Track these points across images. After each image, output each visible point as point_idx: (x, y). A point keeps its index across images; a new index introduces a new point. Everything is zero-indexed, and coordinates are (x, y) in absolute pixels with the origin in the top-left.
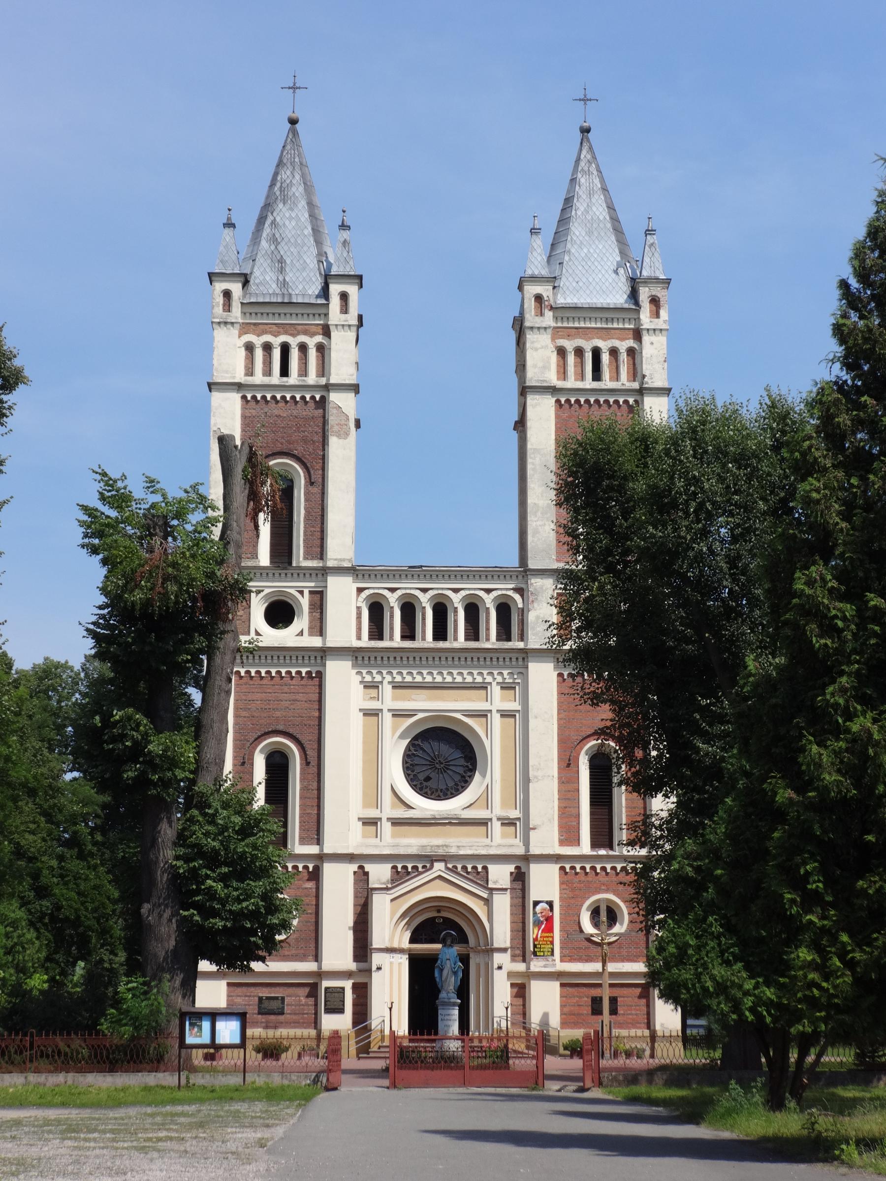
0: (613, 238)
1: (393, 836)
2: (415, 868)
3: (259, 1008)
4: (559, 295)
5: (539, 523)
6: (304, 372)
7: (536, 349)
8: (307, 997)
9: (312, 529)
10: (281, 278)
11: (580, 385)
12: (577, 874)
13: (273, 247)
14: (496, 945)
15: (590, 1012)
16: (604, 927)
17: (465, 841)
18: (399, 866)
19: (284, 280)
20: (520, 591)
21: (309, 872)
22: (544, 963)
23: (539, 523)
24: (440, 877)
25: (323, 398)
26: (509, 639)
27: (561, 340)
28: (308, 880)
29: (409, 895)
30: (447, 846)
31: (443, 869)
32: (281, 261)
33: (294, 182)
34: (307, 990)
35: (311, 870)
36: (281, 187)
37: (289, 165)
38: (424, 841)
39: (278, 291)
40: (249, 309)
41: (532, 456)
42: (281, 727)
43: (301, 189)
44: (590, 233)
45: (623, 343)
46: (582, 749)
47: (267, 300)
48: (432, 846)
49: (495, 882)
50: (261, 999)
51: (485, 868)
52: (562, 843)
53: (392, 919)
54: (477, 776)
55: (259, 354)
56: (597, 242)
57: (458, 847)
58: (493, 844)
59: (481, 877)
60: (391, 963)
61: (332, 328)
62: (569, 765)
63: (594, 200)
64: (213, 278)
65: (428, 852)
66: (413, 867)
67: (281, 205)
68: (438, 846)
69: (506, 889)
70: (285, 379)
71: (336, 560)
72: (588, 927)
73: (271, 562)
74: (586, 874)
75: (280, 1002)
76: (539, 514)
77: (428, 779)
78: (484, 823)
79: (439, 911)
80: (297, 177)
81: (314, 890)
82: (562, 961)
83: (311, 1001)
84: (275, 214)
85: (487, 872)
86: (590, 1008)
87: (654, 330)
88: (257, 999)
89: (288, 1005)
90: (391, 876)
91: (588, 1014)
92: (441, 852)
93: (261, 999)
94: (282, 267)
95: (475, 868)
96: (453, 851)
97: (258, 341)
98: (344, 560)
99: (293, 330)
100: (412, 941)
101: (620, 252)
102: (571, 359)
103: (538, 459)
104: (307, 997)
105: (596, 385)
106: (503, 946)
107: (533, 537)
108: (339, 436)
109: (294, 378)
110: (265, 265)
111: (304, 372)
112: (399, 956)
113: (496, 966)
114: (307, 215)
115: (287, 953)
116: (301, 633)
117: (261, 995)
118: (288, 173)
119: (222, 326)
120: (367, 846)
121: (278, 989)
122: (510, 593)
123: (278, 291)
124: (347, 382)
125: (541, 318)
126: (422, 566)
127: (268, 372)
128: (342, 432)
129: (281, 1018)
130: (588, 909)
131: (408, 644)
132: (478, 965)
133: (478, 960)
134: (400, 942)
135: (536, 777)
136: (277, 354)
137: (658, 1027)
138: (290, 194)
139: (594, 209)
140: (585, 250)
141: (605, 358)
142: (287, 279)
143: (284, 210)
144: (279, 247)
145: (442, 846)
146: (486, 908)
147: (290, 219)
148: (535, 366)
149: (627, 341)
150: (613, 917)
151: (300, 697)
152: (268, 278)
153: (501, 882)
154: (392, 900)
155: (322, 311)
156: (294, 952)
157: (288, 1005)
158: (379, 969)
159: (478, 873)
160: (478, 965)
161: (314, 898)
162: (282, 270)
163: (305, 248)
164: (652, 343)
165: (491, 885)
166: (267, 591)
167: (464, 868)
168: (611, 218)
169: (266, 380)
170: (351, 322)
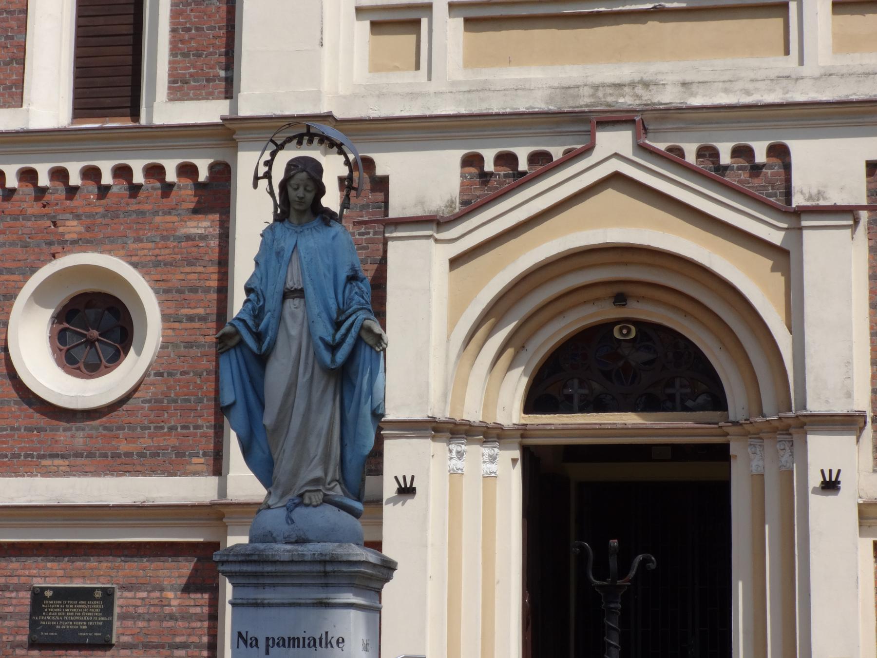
1: (472, 60)
2: (539, 159)
3: (33, 625)
8: (187, 589)
14: (815, 406)
18: (489, 155)
21: (199, 186)
24: (616, 180)
28: (196, 211)
30: (646, 85)
31: (628, 152)
34: (186, 567)
35: (203, 175)
48: (596, 87)
50: (38, 596)
51: (780, 152)
53: (452, 323)
57: (684, 84)
58: (807, 70)
60: (456, 475)
65: (584, 101)
66: (533, 158)
68: (619, 86)
69: (850, 211)
75: (97, 605)
79: (620, 299)
81: (214, 243)
83: (199, 602)
85: (787, 167)
88: (26, 597)
89: (123, 617)
90: (462, 192)
92: (626, 101)
93: (38, 596)
95: (743, 152)
96: (669, 96)
100: (533, 404)
104: (187, 589)
106: (839, 407)
112: (486, 451)
113: (815, 480)
115: (124, 447)
117: (39, 583)
120: (381, 96)
121: (93, 563)
133: (756, 464)
134: (489, 402)
145: (632, 85)
146: (779, 279)
154: (455, 262)
156: (145, 442)
157: (123, 617)
158: (406, 491)
159: (756, 169)
161: (214, 269)
165: (798, 201)
167: (708, 153)
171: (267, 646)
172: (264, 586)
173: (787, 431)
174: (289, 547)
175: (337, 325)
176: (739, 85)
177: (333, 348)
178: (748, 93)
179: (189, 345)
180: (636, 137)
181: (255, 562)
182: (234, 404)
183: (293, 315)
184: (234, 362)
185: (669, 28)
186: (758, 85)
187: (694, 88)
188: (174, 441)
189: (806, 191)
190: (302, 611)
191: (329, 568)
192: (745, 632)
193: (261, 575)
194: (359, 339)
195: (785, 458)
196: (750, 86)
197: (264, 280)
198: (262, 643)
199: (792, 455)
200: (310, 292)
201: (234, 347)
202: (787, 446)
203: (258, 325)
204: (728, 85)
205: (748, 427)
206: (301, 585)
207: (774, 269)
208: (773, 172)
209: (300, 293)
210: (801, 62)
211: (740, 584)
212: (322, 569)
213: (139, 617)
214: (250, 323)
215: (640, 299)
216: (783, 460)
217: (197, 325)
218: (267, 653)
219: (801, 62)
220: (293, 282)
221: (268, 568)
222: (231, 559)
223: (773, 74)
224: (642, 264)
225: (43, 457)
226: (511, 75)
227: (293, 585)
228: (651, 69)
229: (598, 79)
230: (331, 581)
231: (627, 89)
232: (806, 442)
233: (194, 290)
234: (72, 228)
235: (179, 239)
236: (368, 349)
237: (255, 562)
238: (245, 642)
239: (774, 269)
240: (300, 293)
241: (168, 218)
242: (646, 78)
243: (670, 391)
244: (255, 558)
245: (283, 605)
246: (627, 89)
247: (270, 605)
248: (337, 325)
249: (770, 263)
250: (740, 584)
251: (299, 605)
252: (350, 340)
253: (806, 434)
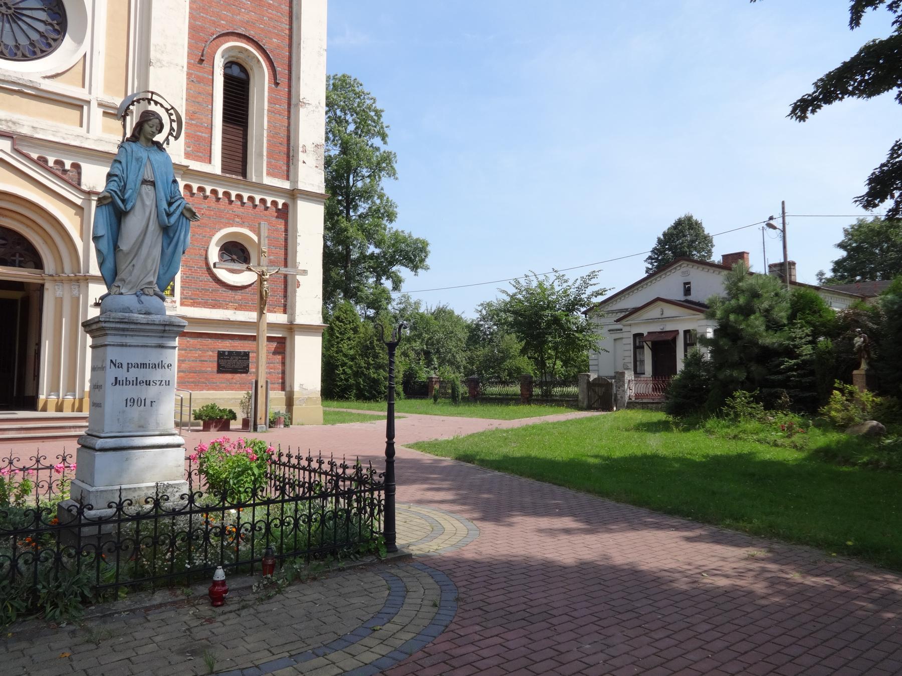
12: (206, 197)
15: (215, 369)
17: (42, 123)
30: (14, 123)
31: (8, 150)
46: (218, 47)
51: (76, 166)
54: (67, 41)
59: (73, 178)
62: (201, 61)
74: (218, 199)
78: (78, 105)
82: (182, 304)
85: (79, 174)
86: (216, 365)
91: (213, 372)
96: (25, 131)
130: (217, 245)
132: (59, 302)
133: (59, 293)
135: (159, 61)
137: (296, 388)
145: (6, 121)
146: (78, 219)
160: (59, 302)
171: (128, 367)
172: (126, 335)
173: (78, 281)
174: (143, 316)
175: (170, 204)
177: (169, 215)
178: (64, 138)
180: (13, 145)
181: (126, 322)
182: (102, 236)
183: (147, 194)
184: (105, 213)
185: (25, 101)
186: (69, 136)
187: (38, 130)
189: (88, 185)
190: (149, 349)
191: (167, 328)
192: (48, 361)
193: (127, 330)
194: (182, 214)
195: (75, 292)
196: (65, 136)
197: (125, 172)
198: (125, 366)
199: (79, 291)
200: (159, 184)
201: (105, 205)
202: (76, 287)
203: (123, 195)
204: (55, 133)
205: (57, 278)
206: (148, 336)
207: (76, 214)
208: (73, 174)
209: (153, 184)
210: (88, 132)
211: (47, 342)
212: (163, 328)
214: (119, 193)
216: (74, 293)
218: (128, 371)
219: (88, 132)
220: (149, 176)
221: (132, 326)
222: (111, 320)
224: (11, 202)
227: (144, 336)
228: (15, 117)
230: (165, 335)
231: (3, 122)
232: (88, 286)
236: (184, 219)
237: (126, 322)
238: (115, 365)
239: (76, 214)
240: (153, 184)
242: (14, 120)
243: (14, 258)
244: (126, 320)
245: (138, 346)
246: (3, 122)
247: (130, 346)
248: (170, 204)
249: (74, 211)
250: (47, 342)
251: (147, 346)
252: (178, 213)
253: (88, 283)
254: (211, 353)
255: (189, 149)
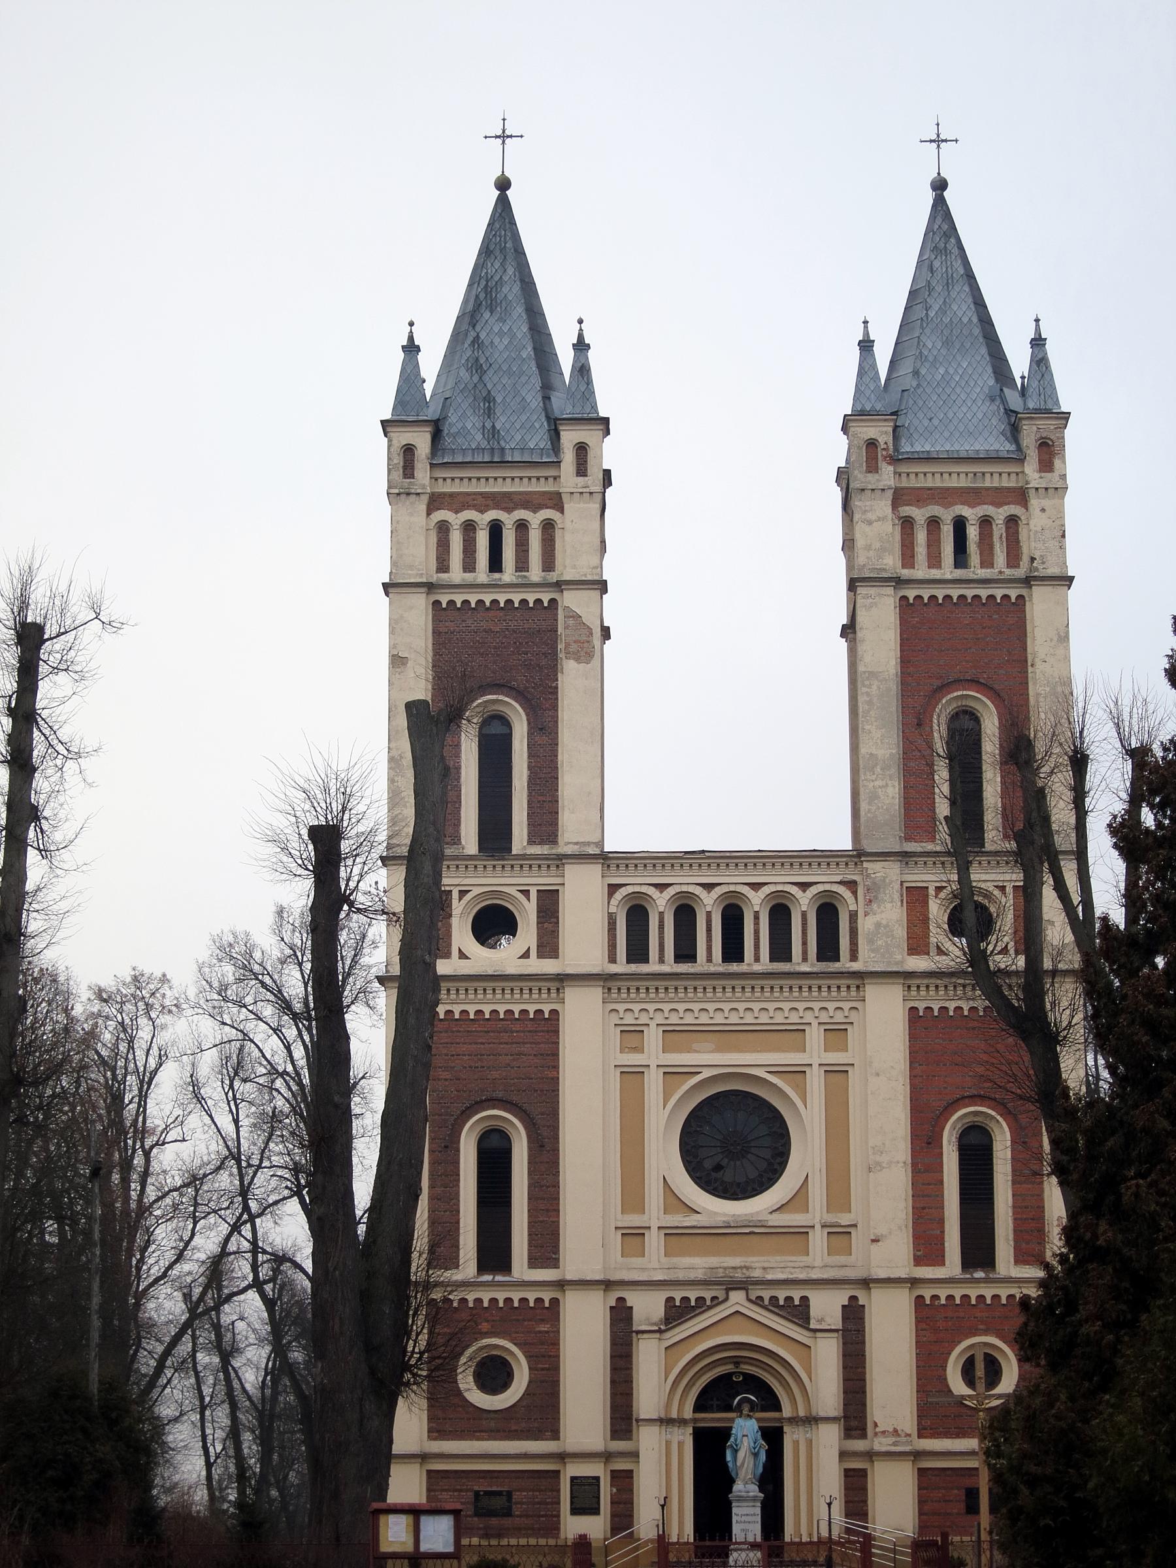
0: (984, 350)
3: (476, 1507)
4: (903, 441)
5: (877, 783)
6: (522, 564)
7: (870, 523)
9: (540, 798)
10: (488, 425)
11: (935, 574)
13: (476, 378)
16: (981, 1385)
17: (774, 1260)
19: (493, 426)
20: (851, 885)
22: (894, 1439)
23: (877, 783)
25: (553, 601)
26: (646, 960)
27: (907, 508)
29: (691, 1340)
30: (747, 1268)
32: (489, 399)
33: (506, 278)
36: (487, 285)
37: (497, 253)
38: (713, 1261)
39: (484, 444)
40: (440, 473)
41: (867, 683)
42: (500, 1094)
43: (516, 288)
44: (947, 343)
45: (1001, 510)
46: (947, 1120)
47: (469, 459)
48: (725, 1268)
49: (820, 1321)
50: (477, 1494)
51: (805, 1299)
52: (918, 1261)
55: (456, 540)
56: (959, 357)
57: (764, 1268)
59: (799, 1313)
61: (565, 498)
63: (953, 294)
64: (389, 429)
67: (487, 315)
70: (497, 575)
71: (576, 843)
72: (959, 1387)
73: (481, 849)
75: (505, 1498)
76: (878, 770)
77: (718, 1168)
78: (802, 1233)
80: (510, 271)
84: (478, 328)
87: (1046, 489)
88: (471, 1495)
92: (739, 1275)
94: (489, 407)
96: (757, 1274)
97: (456, 520)
98: (588, 844)
99: (507, 501)
100: (699, 1407)
101: (995, 372)
102: (921, 536)
103: (875, 687)
105: (959, 573)
107: (869, 804)
108: (578, 660)
109: (509, 574)
110: (465, 405)
111: (522, 564)
114: (525, 328)
116: (526, 955)
117: (476, 1488)
118: (497, 265)
119: (403, 497)
120: (629, 1269)
122: (835, 888)
123: (484, 444)
124: (589, 578)
125: (876, 476)
126: (703, 852)
127: (469, 565)
128: (582, 654)
129: (507, 1522)
131: (634, 968)
132: (796, 1443)
133: (795, 1437)
136: (483, 540)
138: (500, 297)
139: (954, 306)
140: (942, 370)
141: (972, 532)
142: (498, 426)
143: (492, 321)
144: (486, 378)
145: (741, 1268)
147: (501, 334)
148: (868, 548)
149: (1006, 507)
150: (994, 1371)
151: (526, 1048)
152: (469, 426)
153: (828, 1320)
155: (551, 472)
160: (796, 1443)
162: (489, 413)
163: (524, 379)
164: (1043, 510)
166: (476, 891)
168: (980, 320)
169: (469, 577)
170: (593, 489)
176: (788, 1270)
179: (542, 1382)
188: (536, 1425)
213: (523, 1503)
215: (745, 1363)
217: (545, 1372)
223: (802, 1264)
225: (476, 1431)
226: (687, 1261)
229: (725, 1265)
233: (544, 1356)
234: (485, 1326)
235: (536, 1333)
241: (530, 1323)
242: (747, 1264)
254: (956, 1491)
255: (919, 1253)
